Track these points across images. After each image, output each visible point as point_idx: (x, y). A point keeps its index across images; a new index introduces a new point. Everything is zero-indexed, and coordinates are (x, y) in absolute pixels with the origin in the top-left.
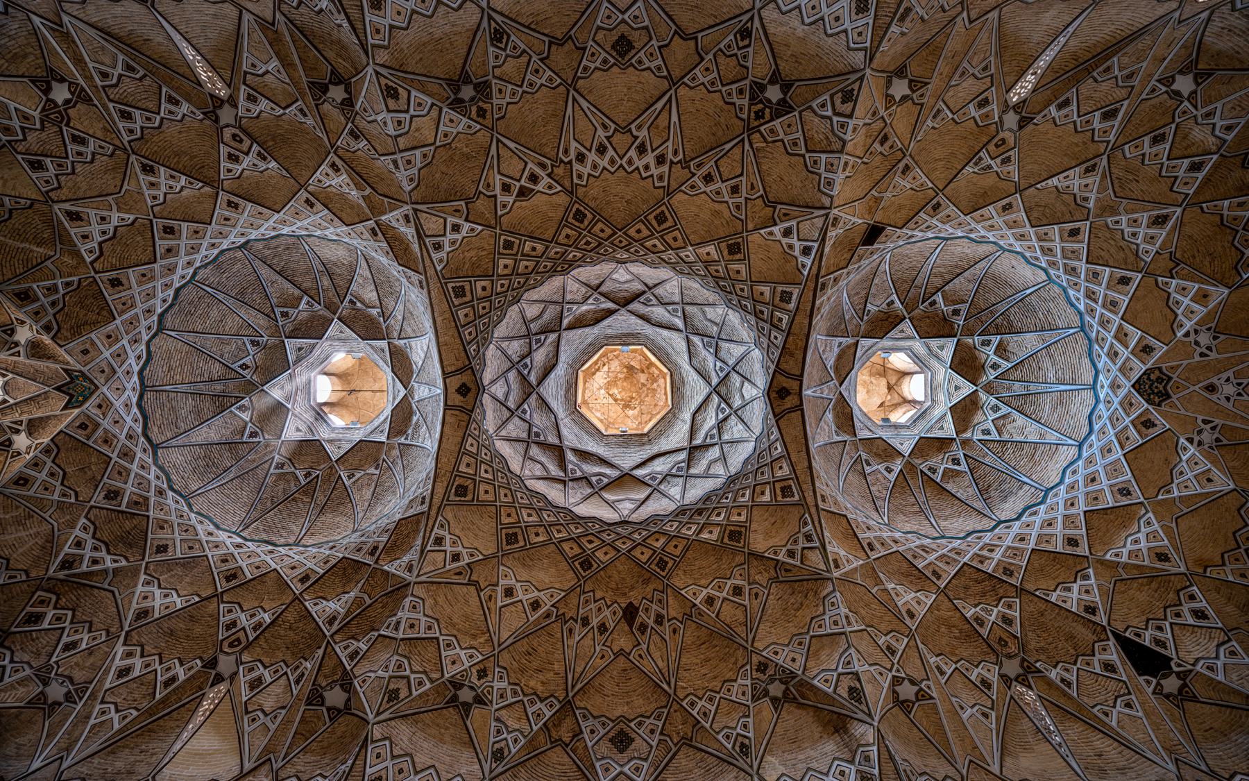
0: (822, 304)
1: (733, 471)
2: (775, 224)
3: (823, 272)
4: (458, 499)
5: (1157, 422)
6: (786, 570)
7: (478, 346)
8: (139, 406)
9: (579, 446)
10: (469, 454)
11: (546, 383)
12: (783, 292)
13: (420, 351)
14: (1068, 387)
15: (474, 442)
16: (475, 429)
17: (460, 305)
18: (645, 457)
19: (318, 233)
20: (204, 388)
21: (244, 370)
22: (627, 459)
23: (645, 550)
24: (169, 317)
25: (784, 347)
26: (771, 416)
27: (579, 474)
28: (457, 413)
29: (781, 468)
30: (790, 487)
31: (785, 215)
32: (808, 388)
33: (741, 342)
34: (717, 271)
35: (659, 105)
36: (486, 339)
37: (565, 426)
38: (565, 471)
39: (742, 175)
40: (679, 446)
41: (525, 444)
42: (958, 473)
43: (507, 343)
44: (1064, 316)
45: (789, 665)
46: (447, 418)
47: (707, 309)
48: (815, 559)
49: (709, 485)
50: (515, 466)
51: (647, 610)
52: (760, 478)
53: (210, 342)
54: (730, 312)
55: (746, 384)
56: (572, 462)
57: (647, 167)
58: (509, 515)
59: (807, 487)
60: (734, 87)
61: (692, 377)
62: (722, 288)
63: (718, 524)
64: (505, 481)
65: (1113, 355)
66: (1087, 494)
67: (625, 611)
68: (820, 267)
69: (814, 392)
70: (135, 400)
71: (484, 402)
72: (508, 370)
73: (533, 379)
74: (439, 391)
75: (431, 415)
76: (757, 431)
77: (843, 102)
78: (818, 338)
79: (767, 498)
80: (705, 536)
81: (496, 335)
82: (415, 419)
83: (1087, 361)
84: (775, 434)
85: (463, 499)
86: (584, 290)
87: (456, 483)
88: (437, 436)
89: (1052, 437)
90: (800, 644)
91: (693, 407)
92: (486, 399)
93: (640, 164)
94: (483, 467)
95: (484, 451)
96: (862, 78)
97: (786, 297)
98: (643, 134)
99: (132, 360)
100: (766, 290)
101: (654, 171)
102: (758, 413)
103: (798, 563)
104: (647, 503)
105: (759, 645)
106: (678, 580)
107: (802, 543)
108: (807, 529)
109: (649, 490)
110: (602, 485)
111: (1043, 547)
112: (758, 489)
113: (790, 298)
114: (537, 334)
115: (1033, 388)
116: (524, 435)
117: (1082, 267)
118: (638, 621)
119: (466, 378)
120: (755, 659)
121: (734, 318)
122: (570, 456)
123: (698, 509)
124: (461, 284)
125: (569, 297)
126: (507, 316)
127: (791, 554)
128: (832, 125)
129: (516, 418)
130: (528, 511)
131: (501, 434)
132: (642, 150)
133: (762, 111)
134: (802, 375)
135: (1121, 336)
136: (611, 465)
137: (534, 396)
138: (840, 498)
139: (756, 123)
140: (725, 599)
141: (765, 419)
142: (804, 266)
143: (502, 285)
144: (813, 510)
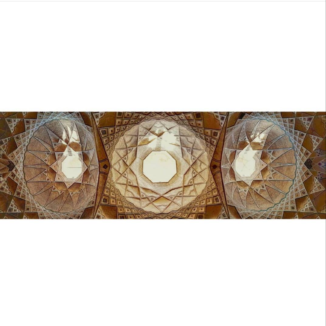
0: (227, 137)
1: (199, 194)
3: (227, 127)
4: (104, 203)
5: (310, 173)
7: (110, 152)
8: (23, 171)
9: (144, 187)
10: (107, 188)
11: (133, 164)
12: (215, 132)
13: (91, 154)
14: (290, 164)
15: (109, 184)
16: (109, 180)
17: (104, 137)
18: (168, 190)
19: (63, 118)
20: (37, 166)
21: (46, 161)
22: (162, 191)
24: (28, 146)
25: (215, 152)
26: (211, 174)
27: (145, 196)
28: (103, 174)
30: (217, 198)
32: (222, 165)
33: (200, 150)
34: (192, 124)
36: (112, 149)
37: (139, 180)
38: (140, 195)
40: (180, 186)
41: (126, 185)
42: (264, 190)
43: (119, 150)
44: (289, 144)
46: (100, 176)
47: (188, 138)
49: (190, 200)
50: (123, 193)
52: (208, 196)
53: (37, 154)
54: (197, 139)
55: (202, 164)
56: (142, 192)
58: (121, 210)
59: (223, 198)
61: (183, 162)
62: (194, 130)
63: (194, 213)
64: (119, 198)
66: (296, 194)
68: (227, 124)
69: (224, 166)
70: (22, 169)
71: (112, 170)
72: (119, 160)
73: (128, 163)
74: (97, 167)
75: (95, 175)
76: (207, 180)
78: (225, 149)
81: (115, 148)
82: (90, 176)
83: (294, 157)
85: (105, 203)
86: (145, 130)
87: (103, 198)
88: (97, 182)
89: (287, 179)
91: (184, 172)
92: (112, 170)
94: (112, 193)
95: (112, 187)
97: (215, 134)
99: (21, 159)
100: (209, 131)
102: (206, 174)
104: (169, 207)
108: (224, 212)
109: (170, 202)
110: (153, 200)
111: (286, 210)
112: (208, 200)
113: (217, 134)
114: (129, 147)
116: (126, 183)
119: (106, 163)
121: (198, 141)
122: (141, 190)
124: (104, 130)
125: (140, 134)
126: (119, 141)
129: (123, 177)
130: (128, 209)
131: (118, 182)
134: (221, 161)
136: (156, 193)
137: (128, 169)
138: (233, 201)
141: (209, 175)
142: (221, 123)
143: (118, 129)
144: (225, 206)
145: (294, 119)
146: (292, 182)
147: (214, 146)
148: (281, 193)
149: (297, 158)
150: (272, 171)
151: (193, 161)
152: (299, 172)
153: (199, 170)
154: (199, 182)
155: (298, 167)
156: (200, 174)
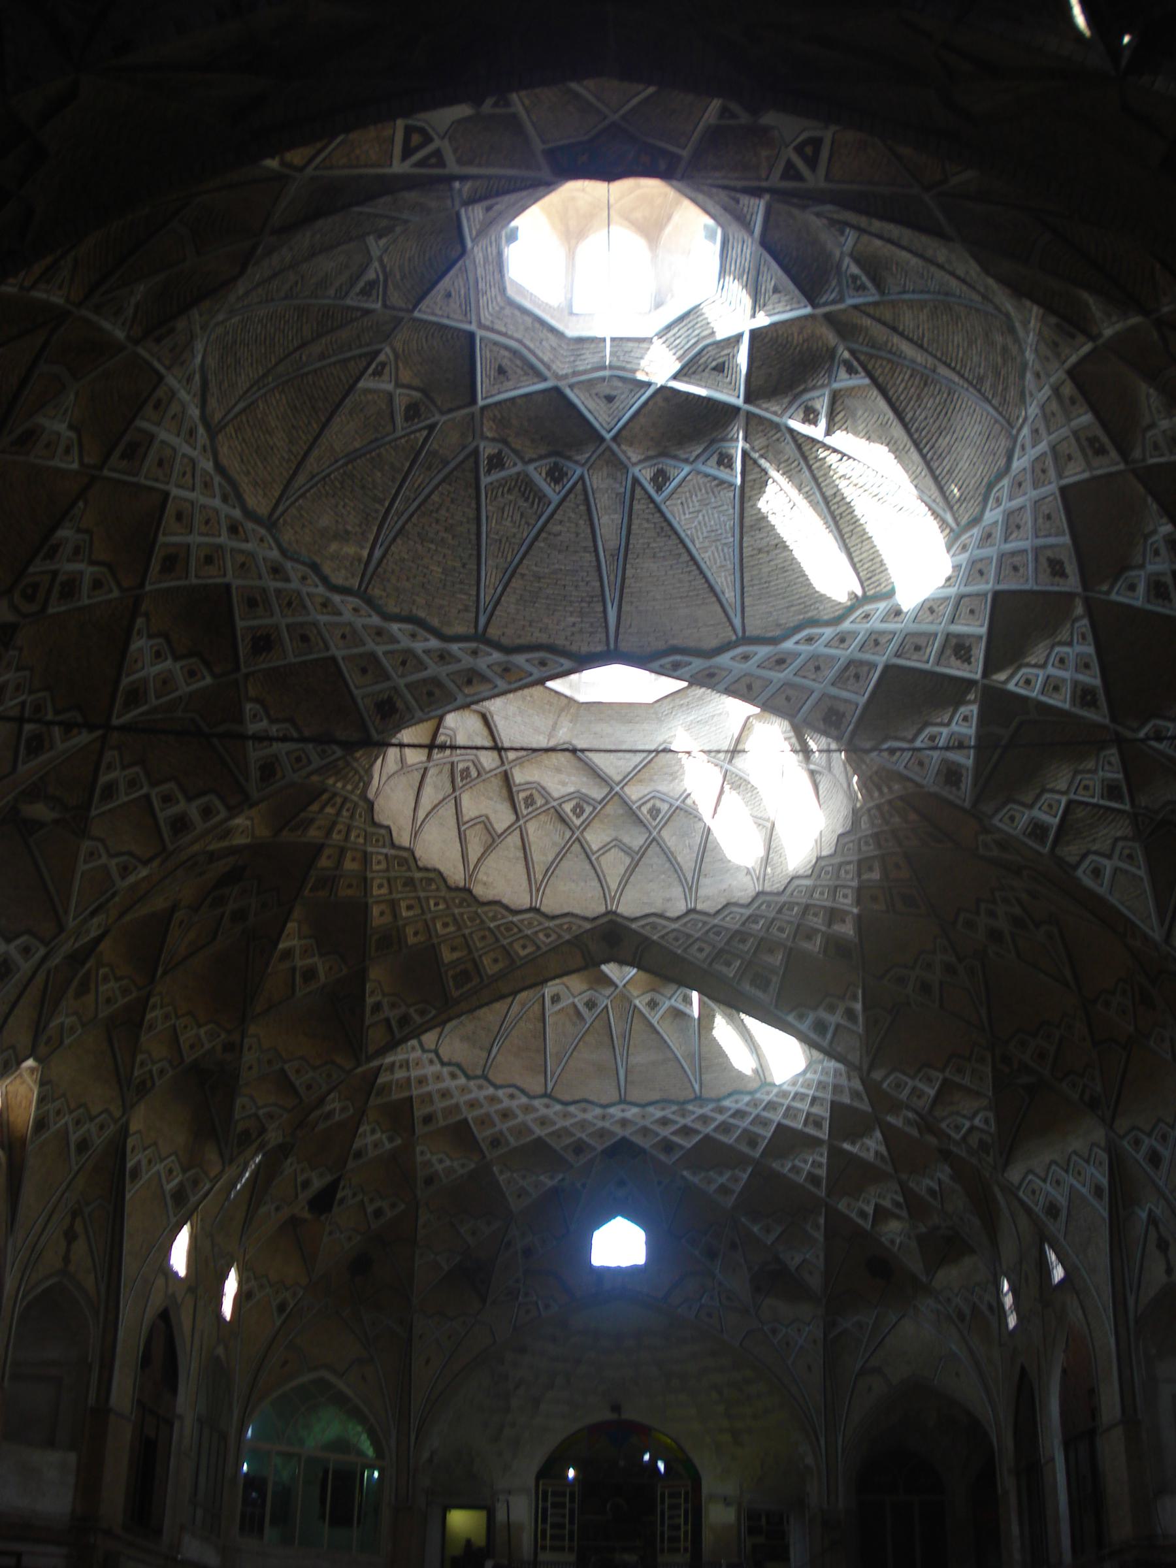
2: (865, 1008)
29: (496, 961)
48: (376, 1036)
65: (664, 1122)
77: (981, 1141)
80: (376, 911)
100: (777, 960)
103: (367, 1023)
105: (252, 1029)
107: (393, 1014)
127: (377, 1007)
128: (964, 1116)
135: (686, 1131)
140: (294, 969)
145: (824, 1134)
146: (539, 1090)
147: (711, 964)
149: (651, 1109)
150: (591, 1005)
151: (645, 809)
152: (589, 1116)
153: (595, 838)
155: (612, 1110)
156: (577, 846)
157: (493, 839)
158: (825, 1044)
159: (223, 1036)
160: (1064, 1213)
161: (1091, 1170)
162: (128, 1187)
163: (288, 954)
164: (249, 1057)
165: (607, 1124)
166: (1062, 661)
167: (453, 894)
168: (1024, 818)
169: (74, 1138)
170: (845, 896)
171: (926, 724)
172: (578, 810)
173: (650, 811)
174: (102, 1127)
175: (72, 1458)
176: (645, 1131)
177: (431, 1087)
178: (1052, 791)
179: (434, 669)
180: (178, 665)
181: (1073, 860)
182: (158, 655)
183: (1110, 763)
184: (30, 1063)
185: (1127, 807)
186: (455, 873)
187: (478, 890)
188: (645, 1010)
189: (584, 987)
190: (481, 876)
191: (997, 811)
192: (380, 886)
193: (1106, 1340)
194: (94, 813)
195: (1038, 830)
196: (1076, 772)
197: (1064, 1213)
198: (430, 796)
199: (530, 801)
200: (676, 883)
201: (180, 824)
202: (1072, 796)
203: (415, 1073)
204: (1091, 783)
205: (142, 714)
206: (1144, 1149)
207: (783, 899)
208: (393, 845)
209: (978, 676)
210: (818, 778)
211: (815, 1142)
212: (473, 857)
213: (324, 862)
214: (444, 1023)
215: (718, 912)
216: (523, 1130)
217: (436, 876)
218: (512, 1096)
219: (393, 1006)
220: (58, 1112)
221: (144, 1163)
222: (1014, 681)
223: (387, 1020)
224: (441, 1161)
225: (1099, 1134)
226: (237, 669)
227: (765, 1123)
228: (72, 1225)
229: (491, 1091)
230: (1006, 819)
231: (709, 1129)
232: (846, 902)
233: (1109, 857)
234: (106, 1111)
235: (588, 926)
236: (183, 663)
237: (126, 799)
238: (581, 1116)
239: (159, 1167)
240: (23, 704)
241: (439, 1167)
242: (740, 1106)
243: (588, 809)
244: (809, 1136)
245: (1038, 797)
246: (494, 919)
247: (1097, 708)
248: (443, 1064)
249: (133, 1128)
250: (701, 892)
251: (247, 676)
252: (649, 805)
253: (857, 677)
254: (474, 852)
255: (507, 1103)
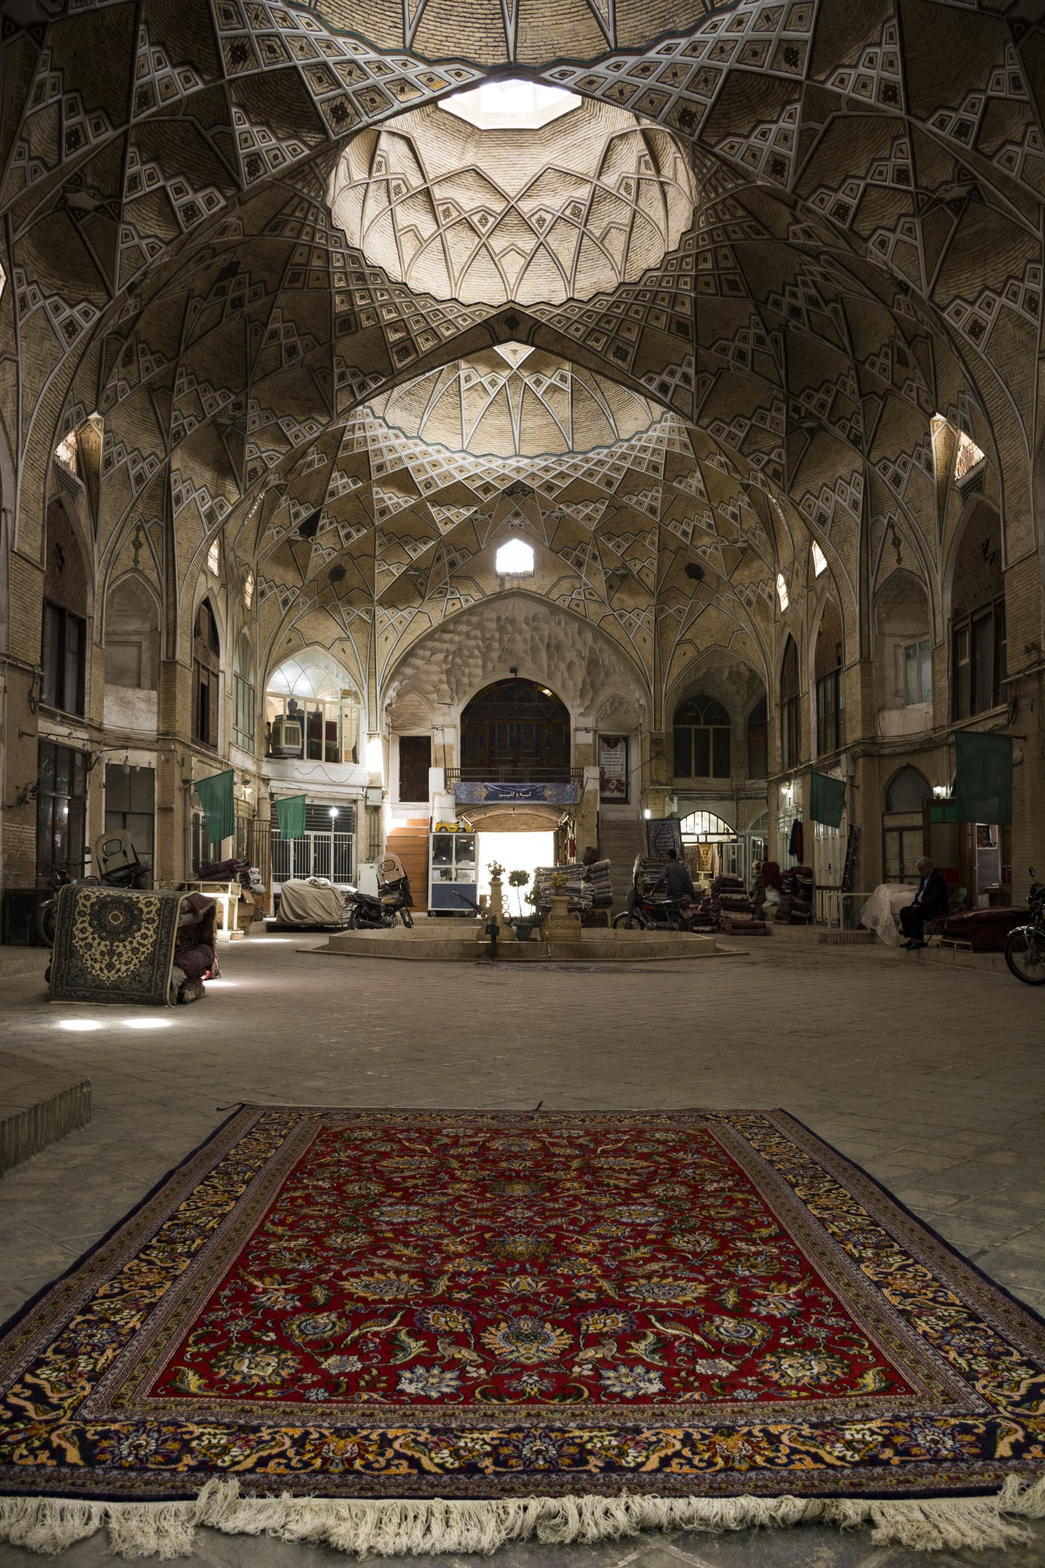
2: (697, 373)
6: (324, 378)
12: (627, 354)
23: (305, 255)
29: (427, 340)
30: (409, 355)
31: (704, 383)
35: (846, 340)
39: (752, 369)
45: (249, 422)
51: (240, 284)
57: (794, 295)
60: (830, 400)
65: (546, 469)
67: (231, 264)
79: (393, 337)
80: (338, 299)
84: (464, 325)
89: (468, 430)
90: (267, 418)
93: (801, 291)
96: (783, 490)
98: (828, 312)
100: (633, 336)
101: (787, 300)
106: (282, 298)
113: (619, 358)
115: (516, 417)
117: (627, 464)
118: (225, 283)
120: (241, 398)
123: (362, 274)
132: (812, 301)
133: (799, 413)
135: (562, 475)
139: (791, 404)
140: (280, 345)
142: (650, 380)
145: (659, 476)
148: (418, 421)
149: (537, 460)
151: (534, 219)
152: (493, 466)
154: (453, 257)
155: (509, 461)
156: (483, 250)
157: (422, 244)
158: (667, 400)
159: (233, 397)
160: (830, 521)
161: (851, 489)
162: (174, 508)
163: (274, 334)
164: (252, 414)
165: (506, 471)
166: (871, 61)
167: (394, 286)
168: (832, 200)
169: (133, 473)
170: (685, 283)
171: (760, 122)
172: (484, 221)
173: (538, 221)
174: (152, 465)
175: (154, 694)
176: (533, 476)
177: (382, 444)
178: (854, 177)
179: (375, 78)
180: (176, 71)
181: (865, 234)
182: (159, 62)
183: (901, 151)
184: (95, 416)
185: (912, 189)
186: (395, 272)
187: (412, 284)
188: (533, 387)
189: (488, 370)
190: (414, 274)
191: (811, 194)
192: (340, 280)
193: (852, 607)
194: (125, 201)
195: (841, 210)
196: (874, 160)
197: (830, 521)
198: (373, 208)
199: (447, 213)
200: (559, 278)
201: (191, 210)
202: (869, 181)
203: (369, 434)
204: (884, 168)
205: (152, 115)
206: (890, 473)
207: (639, 288)
208: (348, 246)
209: (803, 78)
210: (667, 188)
211: (655, 483)
212: (407, 259)
213: (297, 259)
214: (392, 388)
215: (590, 300)
216: (448, 475)
217: (379, 272)
218: (439, 451)
219: (354, 375)
220: (120, 454)
221: (184, 492)
222: (831, 81)
223: (350, 386)
224: (390, 499)
225: (859, 463)
226: (222, 76)
227: (618, 469)
228: (137, 537)
229: (424, 447)
230: (817, 202)
231: (578, 475)
232: (686, 287)
233: (893, 231)
234: (153, 453)
235: (494, 312)
236: (179, 70)
237: (148, 190)
238: (488, 465)
239: (195, 495)
240: (59, 102)
241: (389, 503)
242: (601, 457)
243: (491, 220)
244: (650, 477)
245: (843, 181)
246: (424, 307)
247: (896, 102)
248: (389, 427)
249: (174, 467)
250: (577, 285)
251: (231, 81)
252: (537, 216)
253: (706, 81)
254: (408, 252)
255: (435, 457)
